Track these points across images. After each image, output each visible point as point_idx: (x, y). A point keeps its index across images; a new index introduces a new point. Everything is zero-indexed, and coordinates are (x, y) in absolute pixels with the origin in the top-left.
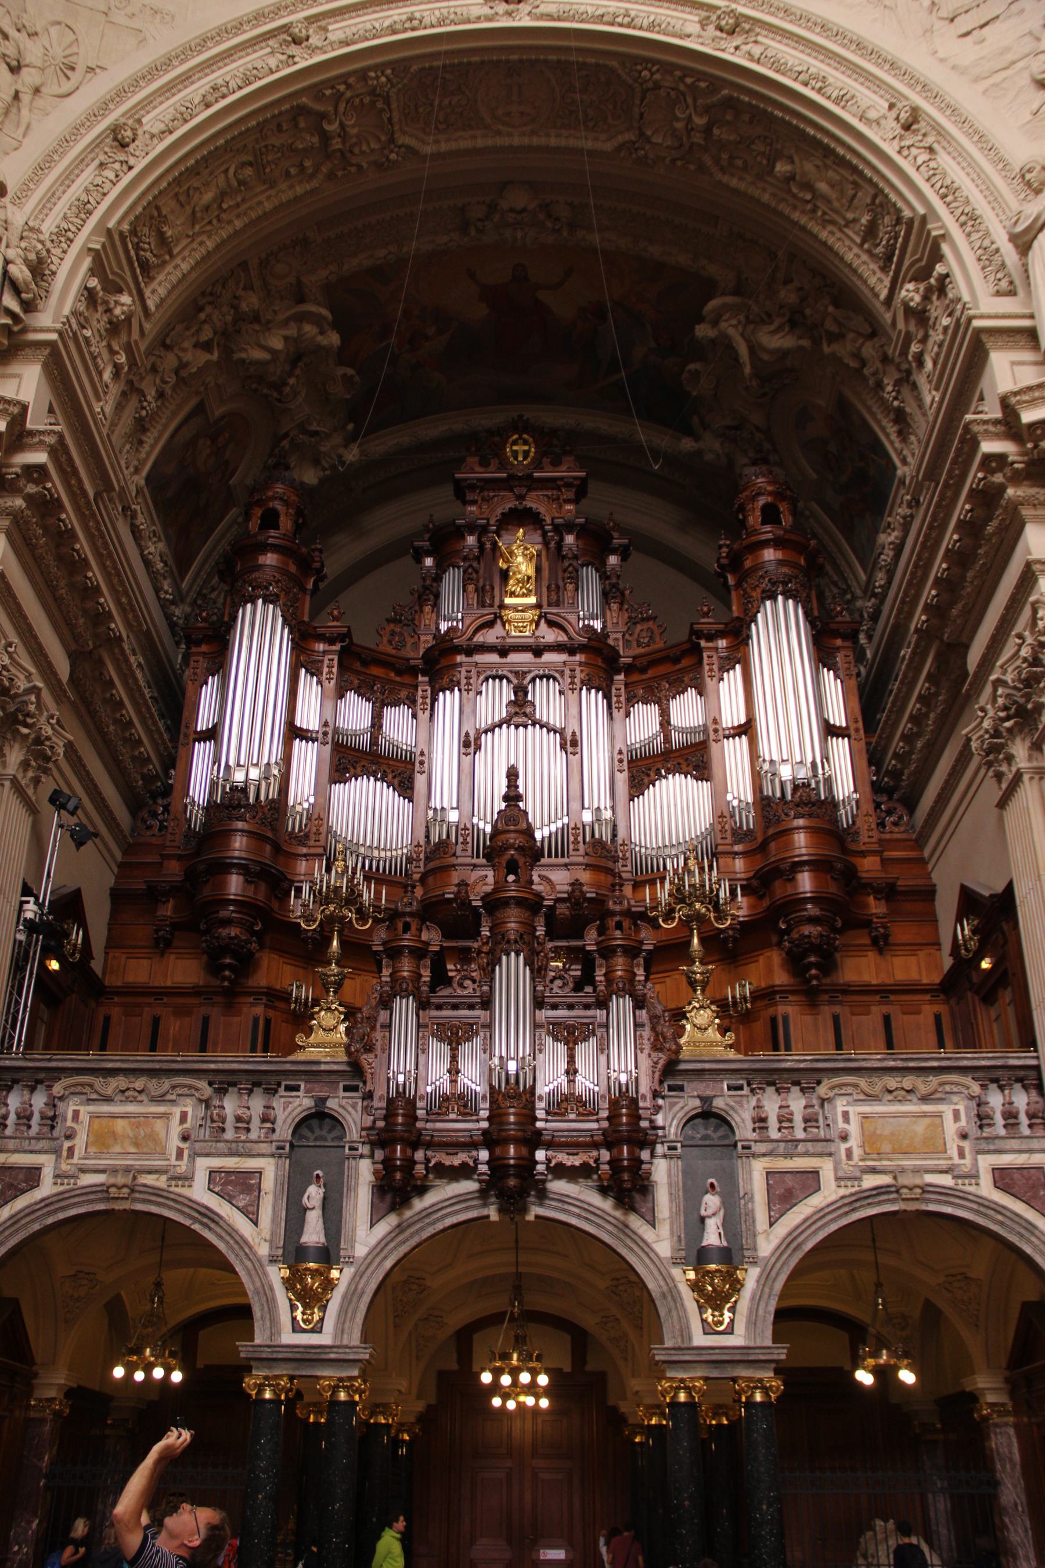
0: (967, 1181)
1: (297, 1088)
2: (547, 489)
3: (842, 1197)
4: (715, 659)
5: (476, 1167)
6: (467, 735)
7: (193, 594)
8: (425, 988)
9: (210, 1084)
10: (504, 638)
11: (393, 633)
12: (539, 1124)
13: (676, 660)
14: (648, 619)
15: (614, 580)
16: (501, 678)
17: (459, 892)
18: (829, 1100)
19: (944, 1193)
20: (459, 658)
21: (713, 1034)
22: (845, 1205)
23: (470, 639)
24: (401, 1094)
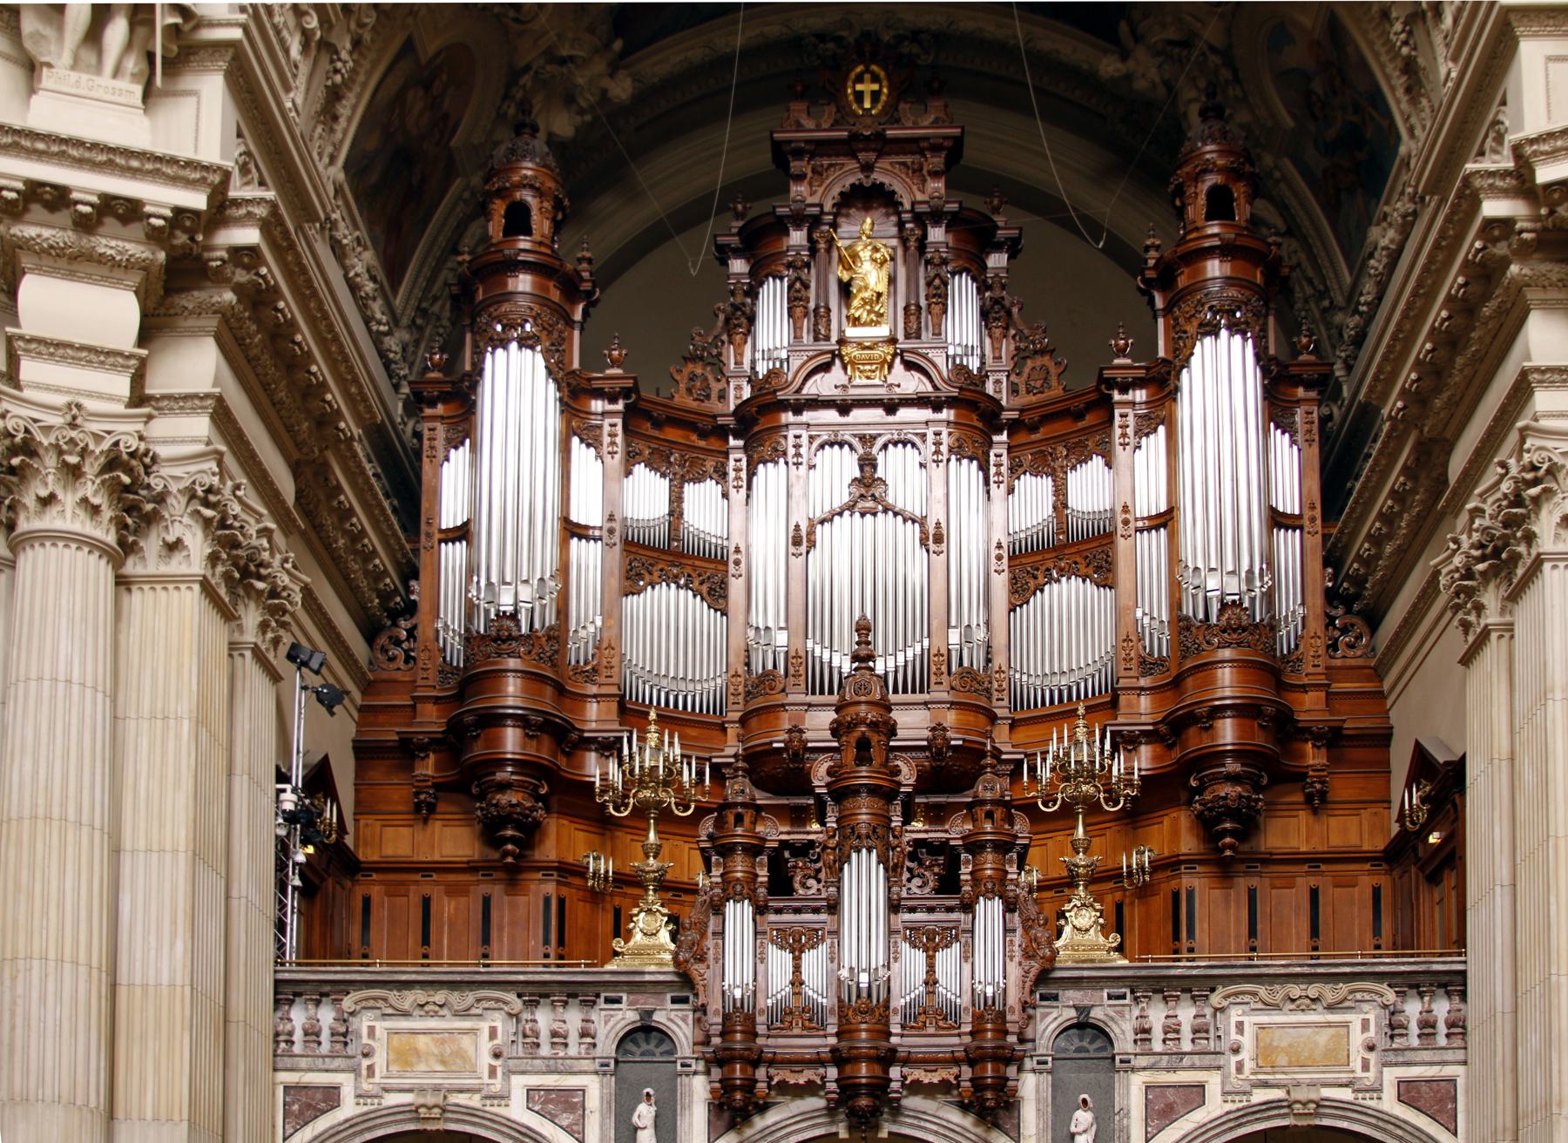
0: (1368, 1095)
1: (618, 1001)
2: (905, 154)
3: (1228, 1113)
4: (1131, 420)
5: (823, 1086)
6: (797, 527)
7: (410, 313)
8: (762, 891)
9: (519, 996)
10: (844, 387)
11: (693, 377)
12: (894, 1040)
13: (1079, 416)
14: (1042, 352)
15: (997, 293)
16: (841, 445)
17: (791, 740)
18: (1222, 1010)
19: (1341, 1107)
20: (788, 417)
21: (1094, 936)
22: (1230, 1120)
23: (799, 391)
24: (739, 1007)
